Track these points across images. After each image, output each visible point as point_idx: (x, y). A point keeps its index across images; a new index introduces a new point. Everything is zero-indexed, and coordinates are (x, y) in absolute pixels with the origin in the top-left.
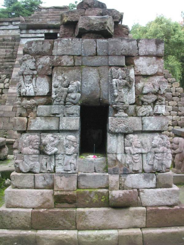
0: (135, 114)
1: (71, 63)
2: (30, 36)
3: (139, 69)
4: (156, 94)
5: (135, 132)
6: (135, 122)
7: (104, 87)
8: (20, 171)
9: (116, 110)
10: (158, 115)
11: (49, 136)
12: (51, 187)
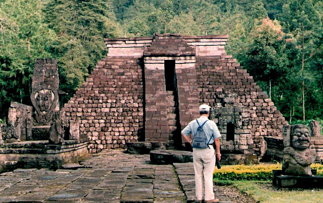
0: (242, 128)
5: (242, 134)
9: (237, 128)
10: (248, 129)
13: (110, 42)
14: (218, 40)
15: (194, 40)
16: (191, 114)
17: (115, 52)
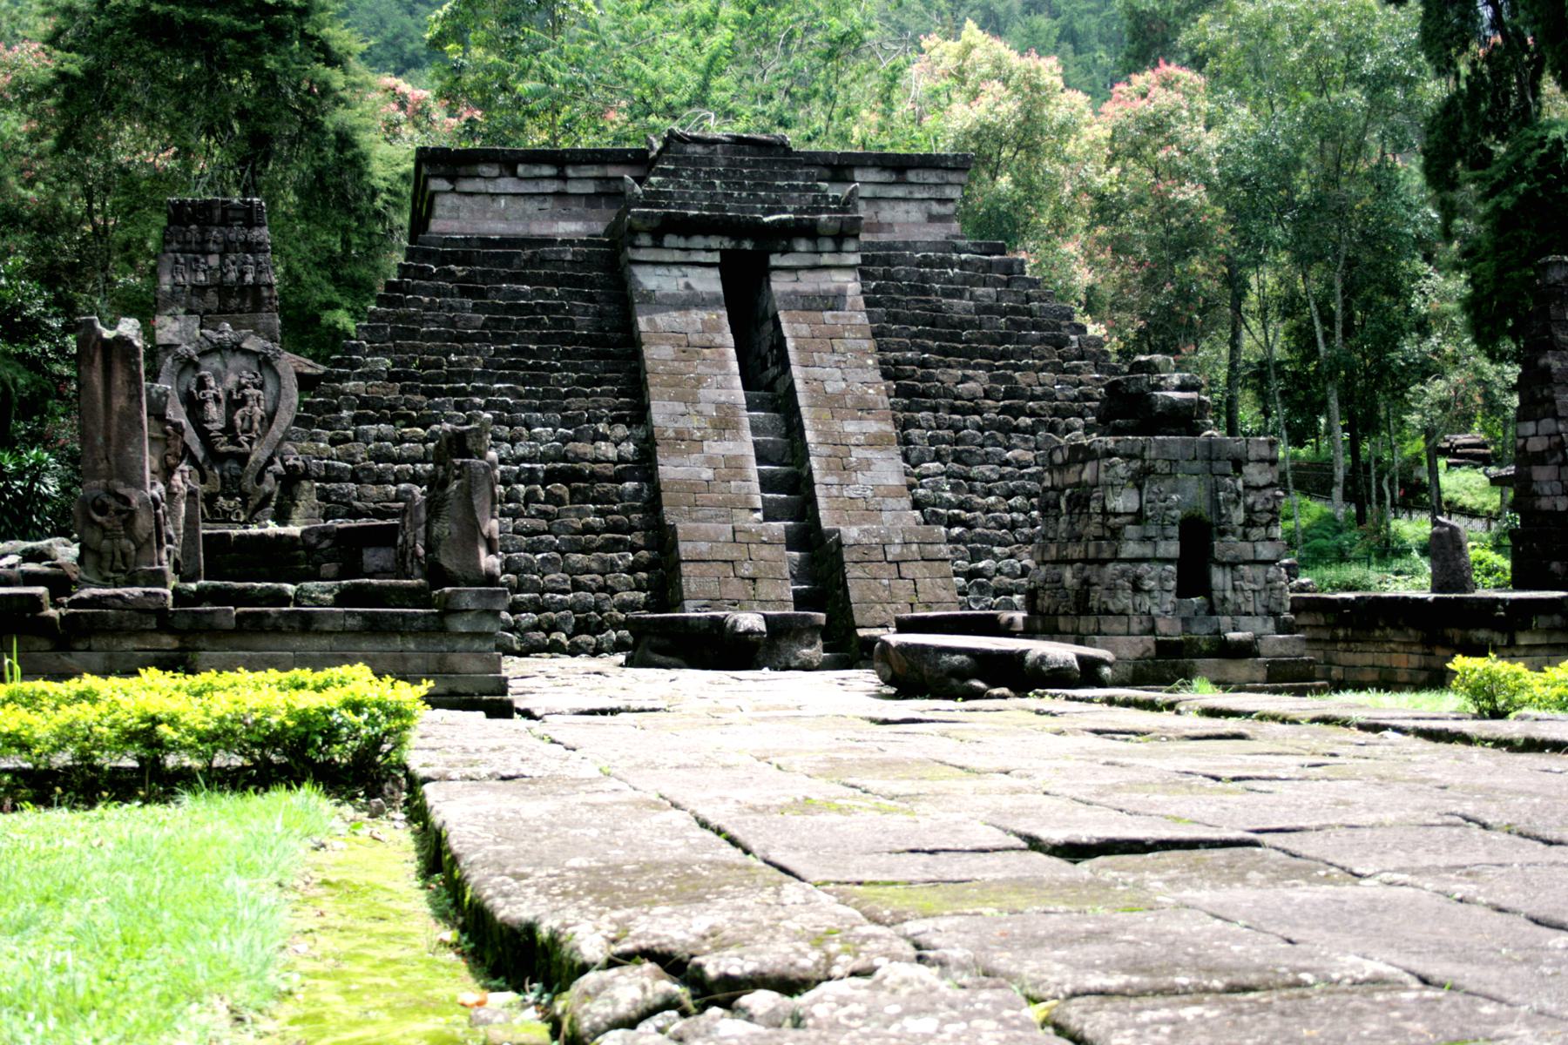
0: (1245, 537)
1: (1167, 470)
2: (666, 256)
5: (1246, 563)
6: (1245, 549)
9: (1223, 533)
10: (1273, 540)
11: (1145, 566)
12: (1152, 631)
14: (932, 177)
15: (827, 173)
16: (869, 493)
17: (464, 214)
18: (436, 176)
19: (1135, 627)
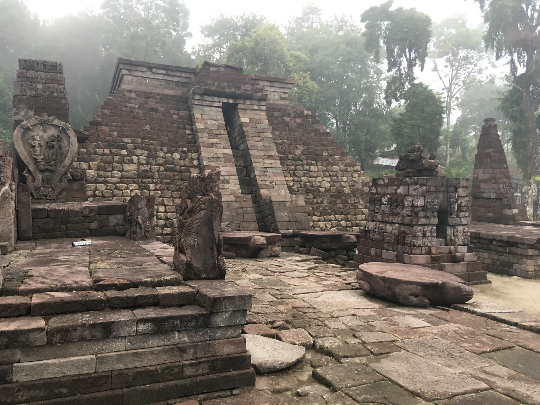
0: (458, 216)
3: (459, 194)
4: (466, 206)
7: (445, 203)
8: (416, 246)
9: (451, 214)
13: (126, 67)
18: (124, 69)
19: (423, 252)
